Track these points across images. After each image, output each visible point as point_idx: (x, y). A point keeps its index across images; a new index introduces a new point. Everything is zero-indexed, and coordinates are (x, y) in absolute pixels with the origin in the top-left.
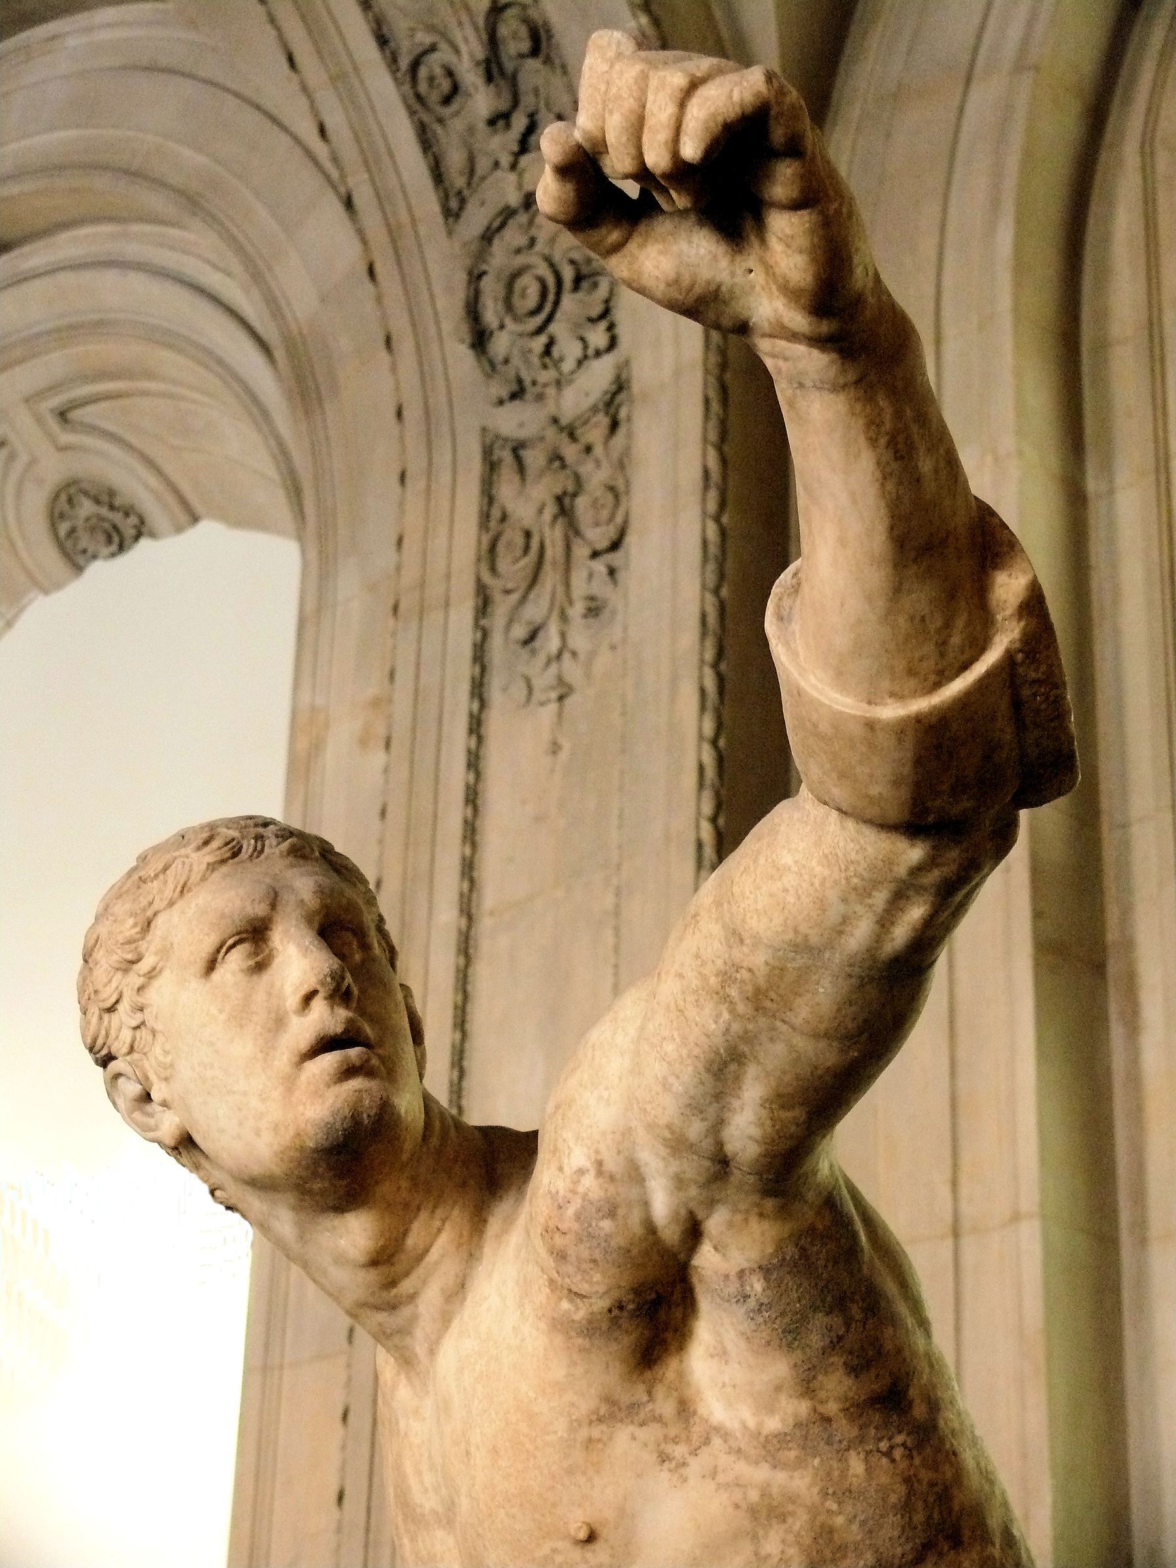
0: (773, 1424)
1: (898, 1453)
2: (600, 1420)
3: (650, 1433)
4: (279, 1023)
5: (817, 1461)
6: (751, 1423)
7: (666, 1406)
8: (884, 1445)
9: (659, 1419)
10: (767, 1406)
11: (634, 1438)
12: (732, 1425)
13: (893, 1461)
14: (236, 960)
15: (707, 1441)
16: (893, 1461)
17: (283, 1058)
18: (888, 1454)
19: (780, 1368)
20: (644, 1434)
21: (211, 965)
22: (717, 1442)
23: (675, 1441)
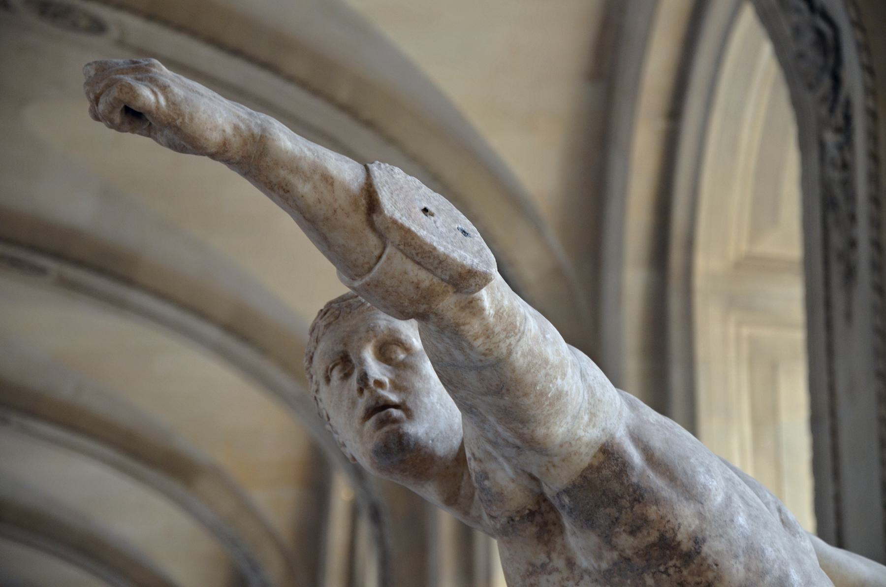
0: (604, 566)
1: (671, 571)
2: (531, 574)
3: (555, 577)
4: (354, 404)
5: (629, 581)
6: (596, 566)
7: (559, 563)
8: (662, 568)
9: (557, 570)
10: (599, 557)
11: (548, 581)
12: (590, 568)
13: (669, 575)
14: (336, 375)
15: (582, 577)
16: (669, 575)
17: (356, 422)
18: (666, 572)
19: (594, 539)
20: (551, 578)
21: (328, 380)
22: (586, 577)
23: (568, 579)
